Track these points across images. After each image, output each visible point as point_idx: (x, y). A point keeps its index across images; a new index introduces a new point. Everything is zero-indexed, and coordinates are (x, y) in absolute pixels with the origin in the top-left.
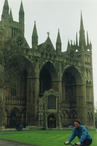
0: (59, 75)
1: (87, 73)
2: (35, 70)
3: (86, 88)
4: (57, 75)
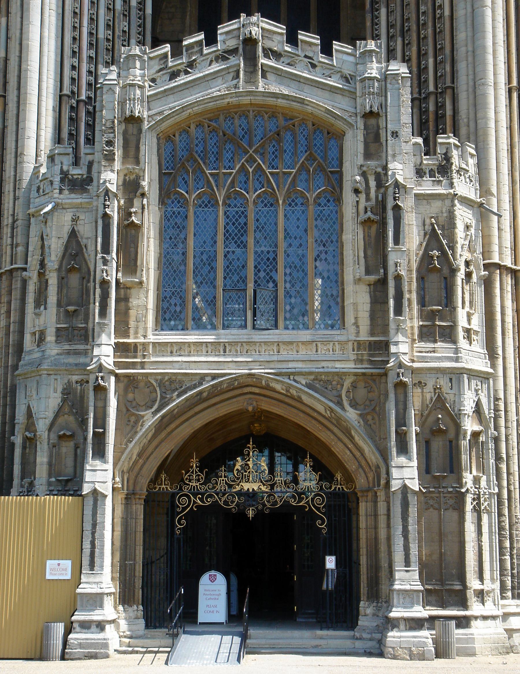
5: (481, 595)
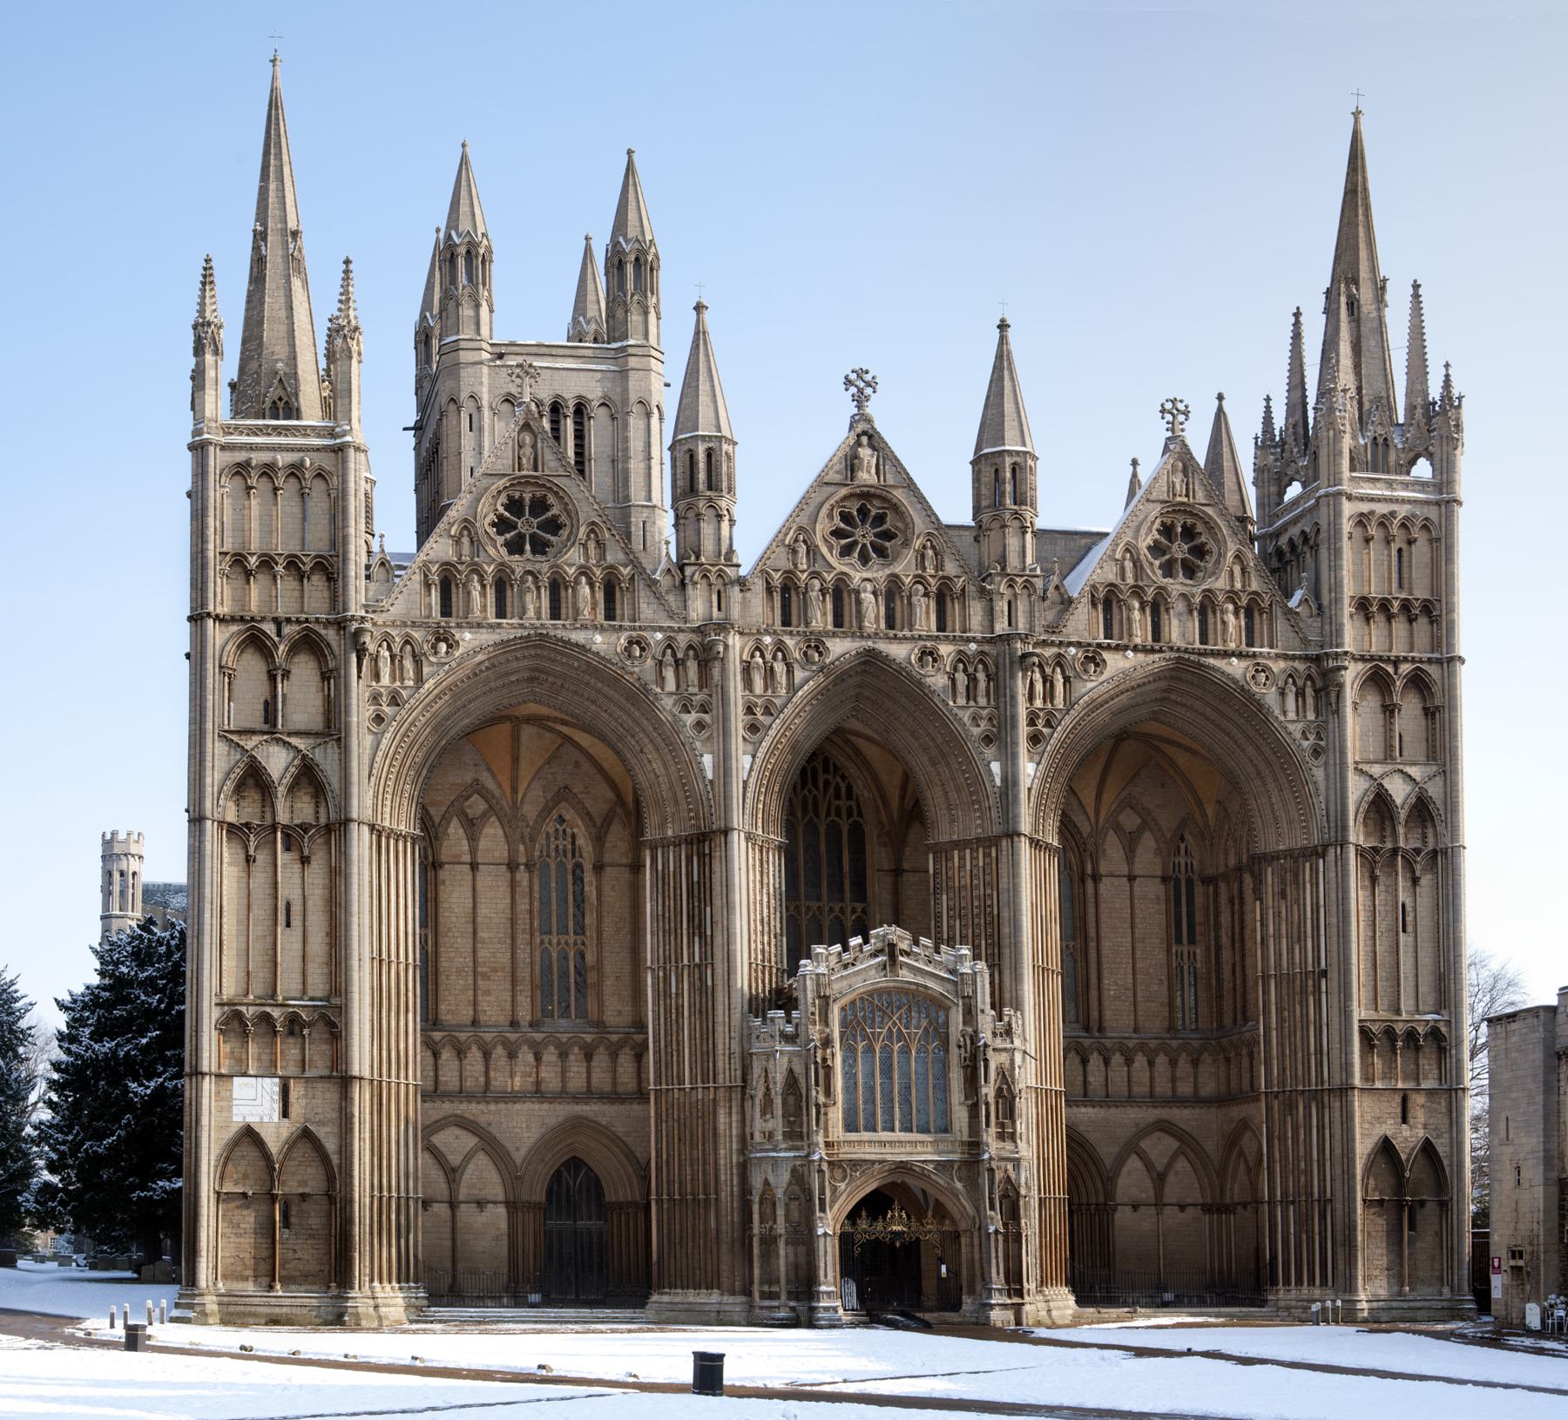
4: (977, 780)
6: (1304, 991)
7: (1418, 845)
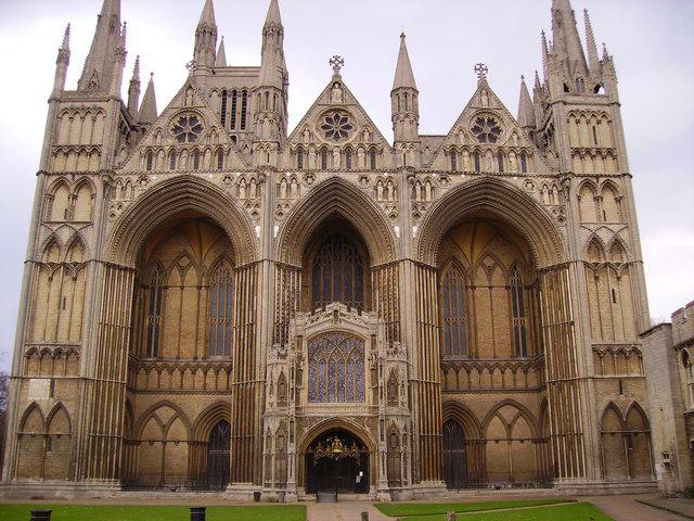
0: (401, 234)
1: (596, 199)
2: (258, 229)
3: (597, 278)
5: (406, 483)
6: (564, 332)
7: (619, 261)
